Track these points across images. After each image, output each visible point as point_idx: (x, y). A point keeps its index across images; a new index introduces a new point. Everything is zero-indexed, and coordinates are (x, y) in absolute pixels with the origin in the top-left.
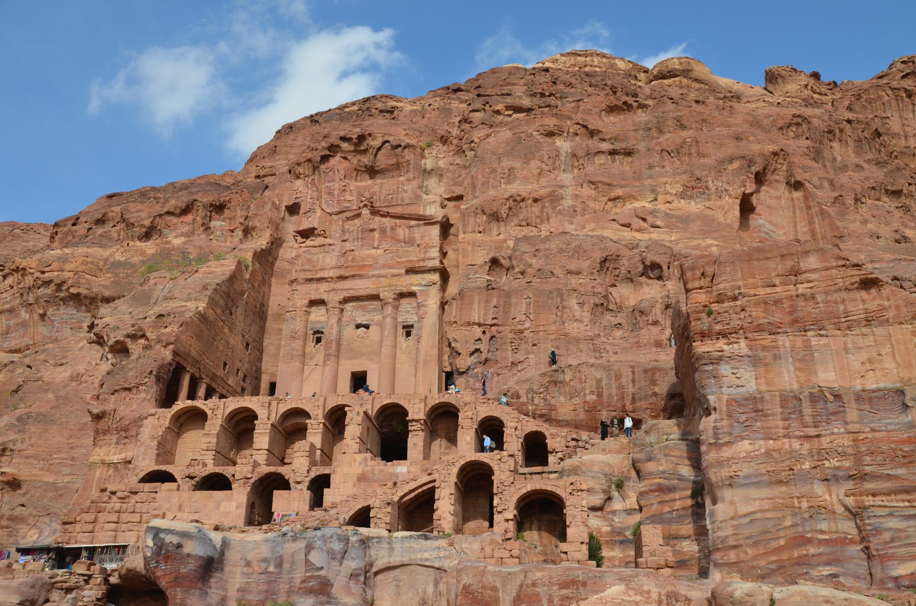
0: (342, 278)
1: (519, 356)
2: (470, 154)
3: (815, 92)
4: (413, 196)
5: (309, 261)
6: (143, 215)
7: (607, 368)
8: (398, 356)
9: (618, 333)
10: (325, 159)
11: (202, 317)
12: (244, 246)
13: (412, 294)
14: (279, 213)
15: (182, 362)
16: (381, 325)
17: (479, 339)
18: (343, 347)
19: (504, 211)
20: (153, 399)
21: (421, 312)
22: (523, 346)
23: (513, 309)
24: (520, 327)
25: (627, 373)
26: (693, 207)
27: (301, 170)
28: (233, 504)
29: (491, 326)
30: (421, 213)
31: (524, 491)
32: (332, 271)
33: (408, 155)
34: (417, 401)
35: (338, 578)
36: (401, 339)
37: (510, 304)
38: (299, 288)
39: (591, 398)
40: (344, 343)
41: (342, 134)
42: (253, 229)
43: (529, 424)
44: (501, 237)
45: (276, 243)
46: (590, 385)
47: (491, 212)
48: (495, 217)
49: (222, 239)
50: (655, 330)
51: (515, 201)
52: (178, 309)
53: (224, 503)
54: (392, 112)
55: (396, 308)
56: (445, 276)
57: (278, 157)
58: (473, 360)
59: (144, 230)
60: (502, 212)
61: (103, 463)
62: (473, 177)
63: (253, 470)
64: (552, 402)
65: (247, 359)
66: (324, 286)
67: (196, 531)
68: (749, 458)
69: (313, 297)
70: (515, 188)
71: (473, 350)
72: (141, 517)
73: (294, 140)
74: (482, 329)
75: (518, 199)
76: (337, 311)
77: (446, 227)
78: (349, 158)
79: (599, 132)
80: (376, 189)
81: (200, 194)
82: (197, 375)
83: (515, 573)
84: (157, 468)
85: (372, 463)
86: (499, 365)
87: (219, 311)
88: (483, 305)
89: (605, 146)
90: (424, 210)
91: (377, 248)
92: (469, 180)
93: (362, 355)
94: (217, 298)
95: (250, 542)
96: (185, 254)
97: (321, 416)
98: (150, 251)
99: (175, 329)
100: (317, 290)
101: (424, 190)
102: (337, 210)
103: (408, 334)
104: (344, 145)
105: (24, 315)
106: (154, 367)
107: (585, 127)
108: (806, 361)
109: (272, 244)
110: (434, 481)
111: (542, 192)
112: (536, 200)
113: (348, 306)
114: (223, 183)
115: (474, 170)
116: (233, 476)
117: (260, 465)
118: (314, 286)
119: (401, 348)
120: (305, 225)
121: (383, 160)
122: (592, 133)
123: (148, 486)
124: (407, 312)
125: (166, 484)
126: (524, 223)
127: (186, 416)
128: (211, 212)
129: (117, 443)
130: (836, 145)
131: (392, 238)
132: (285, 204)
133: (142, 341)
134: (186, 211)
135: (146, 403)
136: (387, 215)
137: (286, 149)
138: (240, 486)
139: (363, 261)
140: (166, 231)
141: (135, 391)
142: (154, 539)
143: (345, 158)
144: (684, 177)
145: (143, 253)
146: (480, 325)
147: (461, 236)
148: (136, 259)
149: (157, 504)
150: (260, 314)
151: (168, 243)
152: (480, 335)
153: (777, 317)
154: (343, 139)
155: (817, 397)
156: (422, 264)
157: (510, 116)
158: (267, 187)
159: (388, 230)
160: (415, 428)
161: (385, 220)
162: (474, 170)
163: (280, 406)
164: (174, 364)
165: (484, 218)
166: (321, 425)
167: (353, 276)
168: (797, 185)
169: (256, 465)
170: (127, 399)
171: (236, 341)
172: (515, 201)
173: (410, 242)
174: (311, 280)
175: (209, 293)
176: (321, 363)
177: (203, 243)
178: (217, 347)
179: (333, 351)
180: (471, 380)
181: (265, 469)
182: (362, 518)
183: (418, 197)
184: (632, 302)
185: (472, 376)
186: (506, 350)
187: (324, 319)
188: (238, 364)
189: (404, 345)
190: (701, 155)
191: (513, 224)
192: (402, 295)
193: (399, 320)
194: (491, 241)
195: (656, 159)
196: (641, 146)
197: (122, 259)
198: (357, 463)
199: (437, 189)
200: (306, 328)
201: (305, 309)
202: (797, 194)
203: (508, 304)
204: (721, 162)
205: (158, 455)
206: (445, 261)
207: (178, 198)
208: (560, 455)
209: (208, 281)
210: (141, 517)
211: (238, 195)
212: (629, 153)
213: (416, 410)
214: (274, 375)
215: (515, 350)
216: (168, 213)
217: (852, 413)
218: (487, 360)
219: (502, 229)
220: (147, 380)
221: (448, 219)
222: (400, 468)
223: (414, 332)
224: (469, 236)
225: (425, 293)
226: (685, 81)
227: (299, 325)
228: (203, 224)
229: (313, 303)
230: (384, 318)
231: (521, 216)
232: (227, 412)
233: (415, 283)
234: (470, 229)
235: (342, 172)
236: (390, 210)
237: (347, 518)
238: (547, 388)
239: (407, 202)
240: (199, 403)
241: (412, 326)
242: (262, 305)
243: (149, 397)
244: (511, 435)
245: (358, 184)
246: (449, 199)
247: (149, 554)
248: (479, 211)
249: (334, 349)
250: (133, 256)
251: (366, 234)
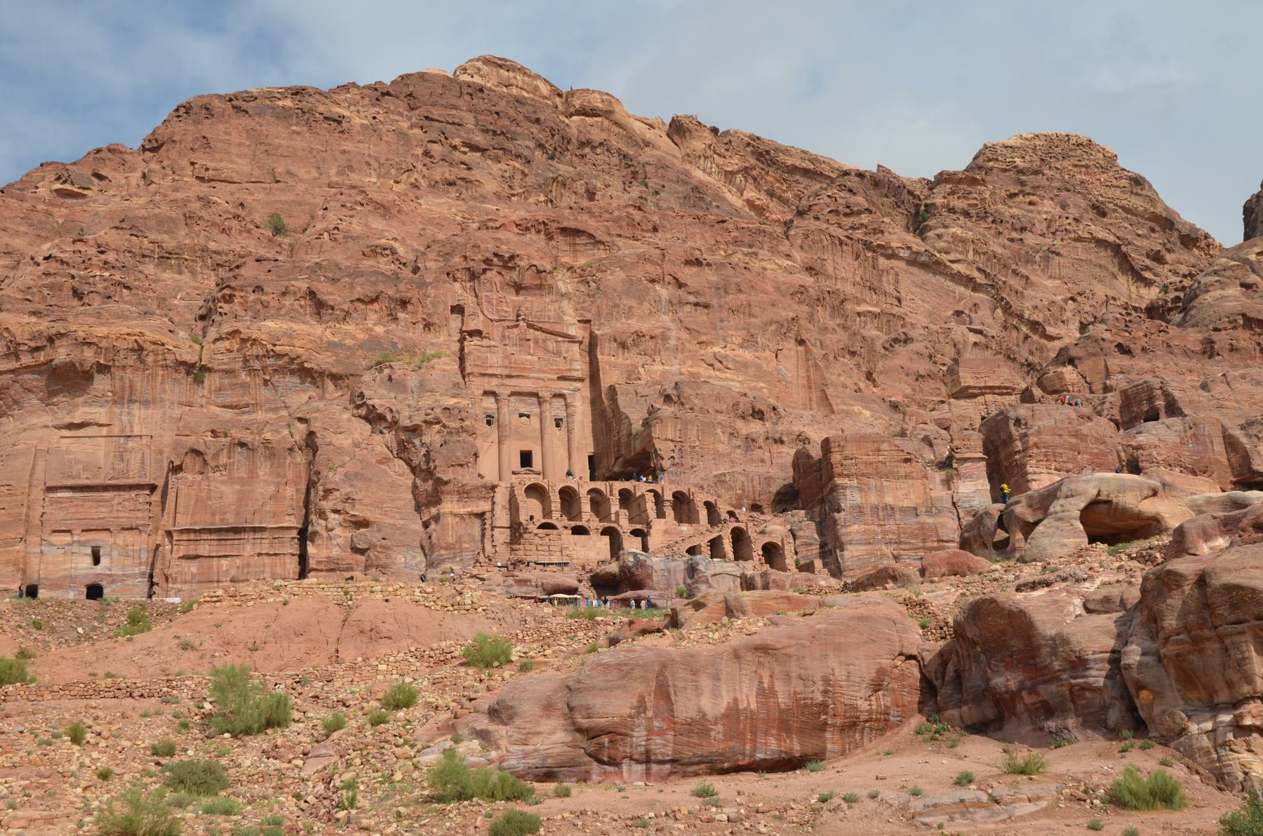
0: (509, 376)
1: (694, 463)
2: (593, 285)
3: (715, 152)
5: (479, 357)
7: (747, 476)
9: (739, 451)
13: (562, 396)
19: (629, 341)
21: (570, 411)
25: (756, 478)
26: (747, 355)
39: (739, 492)
42: (433, 324)
46: (739, 485)
50: (760, 451)
54: (339, 123)
57: (217, 156)
61: (451, 513)
66: (495, 381)
68: (857, 532)
70: (635, 324)
79: (685, 285)
80: (528, 305)
89: (692, 299)
96: (394, 345)
105: (243, 377)
107: (676, 279)
108: (881, 492)
111: (657, 332)
118: (486, 379)
120: (472, 325)
121: (528, 279)
122: (680, 285)
130: (820, 308)
132: (450, 304)
133: (437, 427)
134: (373, 301)
136: (541, 329)
144: (744, 333)
145: (353, 337)
153: (870, 470)
155: (885, 508)
157: (465, 153)
161: (538, 333)
167: (518, 376)
168: (801, 342)
173: (558, 353)
174: (484, 375)
183: (560, 318)
184: (745, 432)
190: (751, 315)
192: (556, 396)
195: (725, 315)
196: (714, 302)
202: (801, 348)
203: (686, 429)
204: (765, 324)
212: (706, 306)
217: (898, 517)
223: (564, 424)
224: (606, 358)
226: (606, 123)
229: (486, 393)
231: (642, 348)
233: (565, 387)
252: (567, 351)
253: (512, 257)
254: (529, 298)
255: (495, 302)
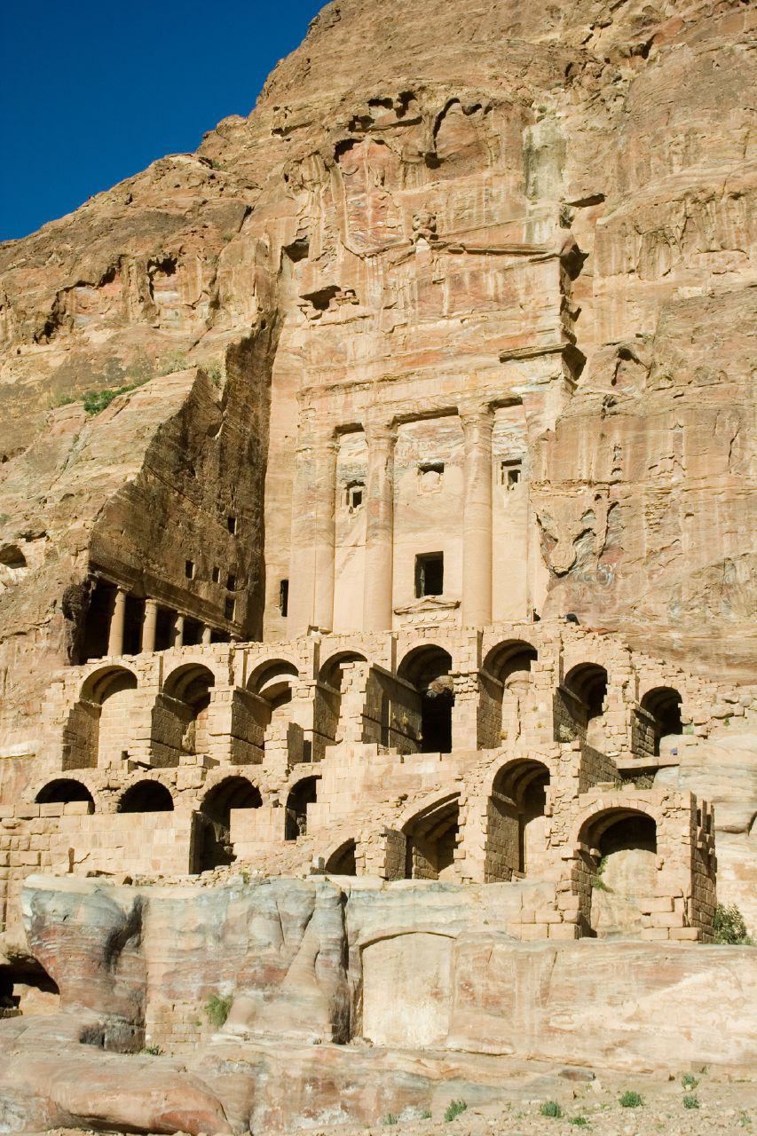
0: (388, 380)
4: (507, 207)
6: (39, 292)
8: (497, 518)
10: (343, 147)
11: (135, 492)
12: (213, 336)
14: (271, 263)
15: (108, 577)
16: (462, 463)
17: (590, 511)
18: (399, 510)
20: (64, 648)
22: (668, 520)
23: (649, 451)
24: (664, 483)
27: (304, 171)
28: (170, 832)
29: (611, 484)
30: (524, 241)
31: (593, 811)
32: (370, 368)
33: (496, 124)
34: (465, 642)
35: (296, 958)
36: (499, 489)
37: (644, 441)
38: (315, 404)
40: (400, 502)
41: (374, 91)
43: (652, 674)
44: (672, 277)
45: (269, 323)
47: (650, 229)
48: (659, 237)
49: (177, 323)
51: (695, 201)
52: (96, 484)
53: (157, 832)
55: (489, 430)
56: (574, 360)
57: (313, 85)
58: (581, 548)
59: (42, 321)
60: (673, 226)
62: (620, 156)
63: (204, 774)
64: (717, 623)
65: (232, 548)
66: (360, 398)
67: (91, 891)
69: (341, 422)
71: (580, 532)
72: (40, 856)
73: (344, 41)
74: (594, 491)
75: (702, 197)
76: (384, 444)
77: (572, 263)
78: (388, 141)
81: (133, 240)
82: (139, 594)
83: (539, 955)
84: (61, 775)
85: (382, 758)
86: (627, 557)
87: (167, 474)
88: (595, 447)
90: (530, 235)
91: (450, 318)
92: (614, 161)
93: (433, 521)
94: (163, 452)
95: (177, 902)
96: (113, 363)
97: (310, 675)
98: (56, 362)
99: (90, 524)
100: (347, 406)
101: (530, 191)
102: (373, 248)
103: (514, 476)
104: (379, 113)
106: (58, 593)
109: (263, 326)
110: (458, 794)
112: (736, 196)
113: (405, 430)
114: (174, 212)
115: (623, 139)
116: (174, 784)
117: (218, 763)
118: (339, 398)
119: (501, 506)
121: (451, 137)
123: (47, 808)
124: (510, 435)
125: (72, 804)
126: (714, 246)
127: (109, 680)
128: (151, 275)
129: (15, 725)
131: (474, 293)
133: (42, 542)
134: (108, 278)
135: (52, 656)
137: (330, 64)
138: (184, 801)
139: (424, 344)
140: (81, 319)
141: (33, 636)
142: (33, 905)
143: (380, 142)
145: (44, 368)
146: (590, 483)
147: (597, 283)
148: (34, 379)
149: (60, 836)
150: (250, 461)
151: (84, 343)
152: (589, 502)
154: (374, 103)
156: (531, 343)
158: (249, 211)
159: (467, 279)
160: (465, 687)
161: (459, 260)
162: (623, 139)
163: (250, 657)
164: (93, 586)
165: (640, 241)
166: (313, 689)
169: (209, 763)
170: (23, 650)
171: (207, 520)
172: (695, 201)
173: (507, 299)
175: (145, 445)
176: (362, 542)
177: (140, 338)
178: (171, 538)
179: (381, 519)
180: (577, 586)
181: (226, 769)
182: (344, 861)
183: (517, 209)
185: (579, 579)
186: (639, 527)
187: (363, 459)
188: (214, 560)
189: (506, 500)
191: (694, 248)
193: (495, 452)
194: (653, 289)
197: (12, 381)
198: (357, 759)
199: (556, 185)
200: (334, 477)
201: (329, 444)
203: (640, 440)
205: (67, 751)
206: (577, 330)
207: (95, 253)
208: (699, 730)
209: (145, 421)
210: (40, 856)
211: (196, 237)
213: (464, 658)
214: (285, 565)
215: (656, 527)
216: (81, 284)
218: (605, 548)
219: (675, 261)
220: (50, 616)
221: (575, 247)
222: (428, 765)
224: (612, 282)
225: (539, 400)
227: (319, 475)
228: (142, 299)
229: (342, 430)
230: (467, 451)
232: (166, 674)
233: (518, 379)
234: (612, 267)
235: (377, 172)
236: (465, 241)
237: (327, 858)
238: (706, 597)
239: (497, 220)
240: (124, 662)
241: (518, 462)
242: (255, 442)
243: (55, 645)
244: (615, 698)
245: (408, 192)
246: (577, 204)
247: (28, 927)
248: (630, 228)
249: (382, 516)
250: (28, 373)
251: (427, 292)
252: (528, 290)
253: (407, 97)
254: (444, 183)
255: (369, 213)
